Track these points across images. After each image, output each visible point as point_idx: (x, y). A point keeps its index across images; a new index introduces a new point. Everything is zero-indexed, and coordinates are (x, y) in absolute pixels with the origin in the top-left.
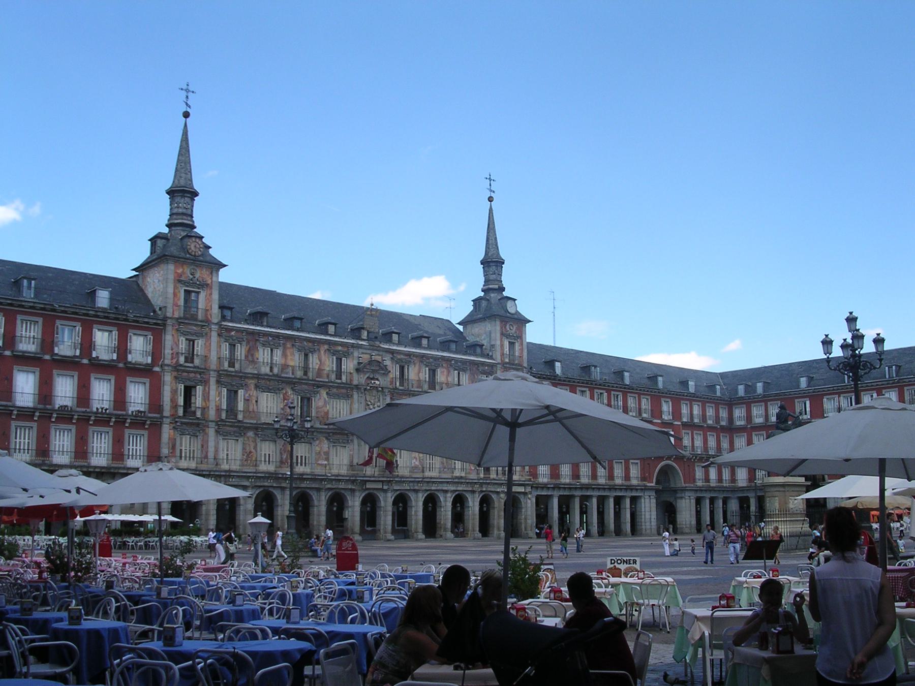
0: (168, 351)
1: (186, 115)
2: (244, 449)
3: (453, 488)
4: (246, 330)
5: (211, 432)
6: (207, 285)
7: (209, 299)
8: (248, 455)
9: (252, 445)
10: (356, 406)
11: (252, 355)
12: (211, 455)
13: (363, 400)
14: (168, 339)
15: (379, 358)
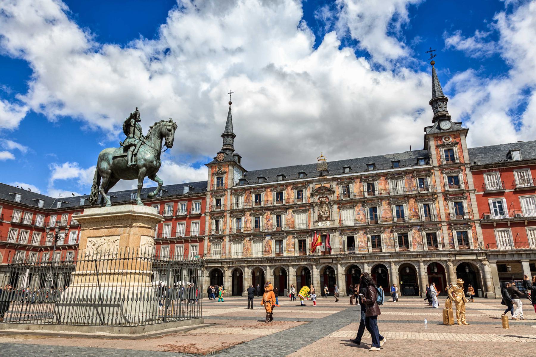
0: (208, 206)
1: (230, 103)
2: (244, 247)
3: (394, 260)
4: (244, 188)
5: (227, 240)
6: (226, 172)
7: (227, 179)
8: (247, 250)
9: (249, 244)
10: (312, 215)
11: (249, 199)
12: (227, 251)
13: (316, 211)
14: (208, 200)
15: (327, 185)
